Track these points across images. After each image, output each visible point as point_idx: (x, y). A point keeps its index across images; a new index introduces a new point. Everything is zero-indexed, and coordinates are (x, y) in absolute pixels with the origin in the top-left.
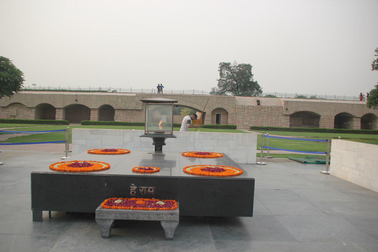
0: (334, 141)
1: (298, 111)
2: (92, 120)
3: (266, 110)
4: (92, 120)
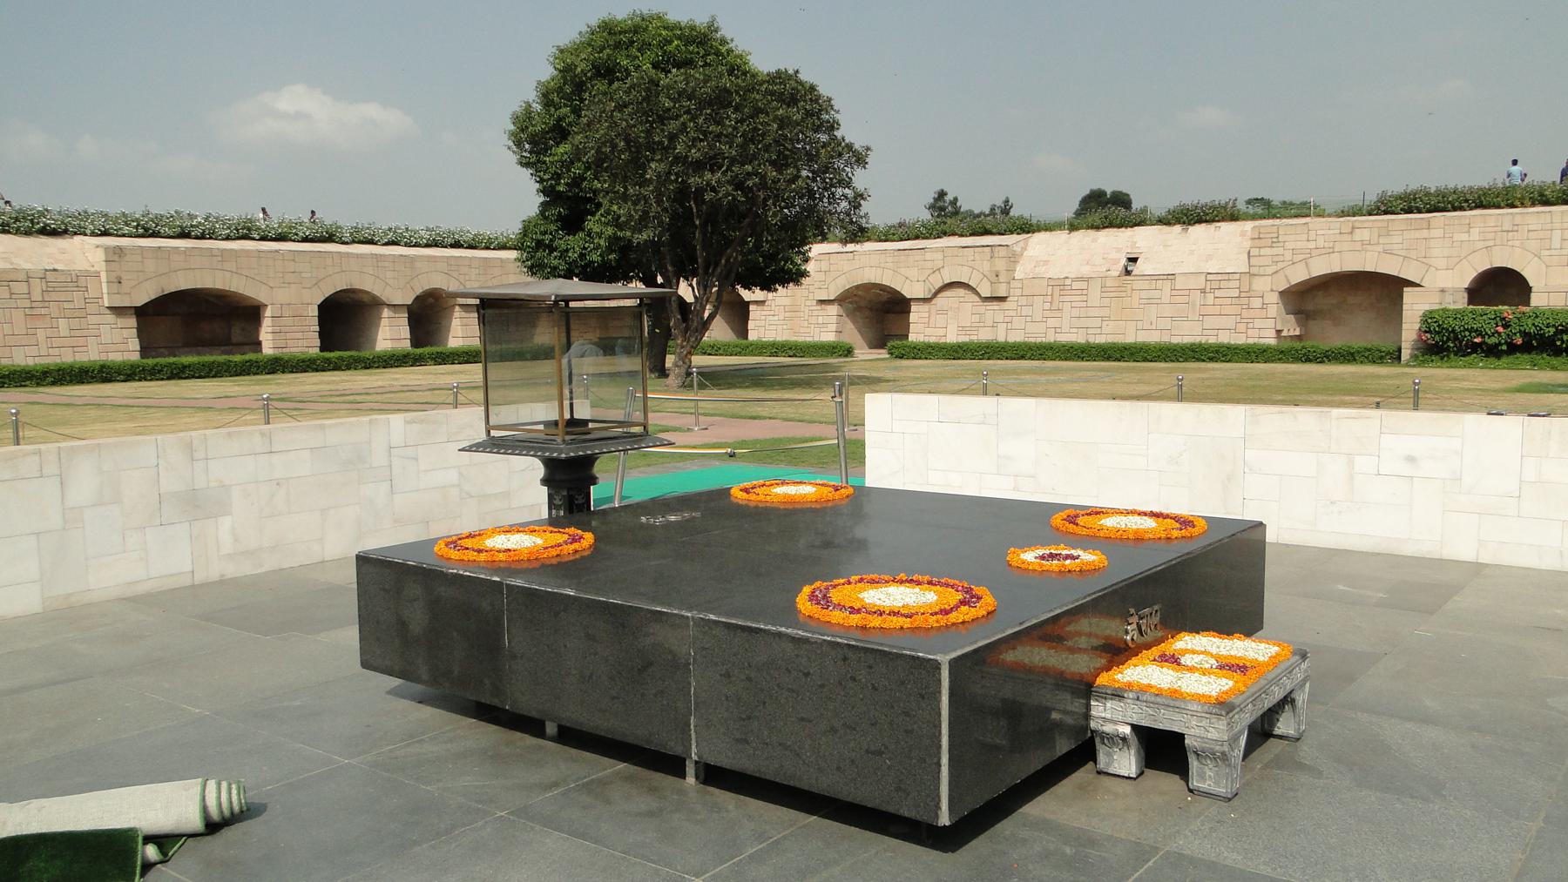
0: (867, 396)
1: (172, 288)
3: (21, 288)
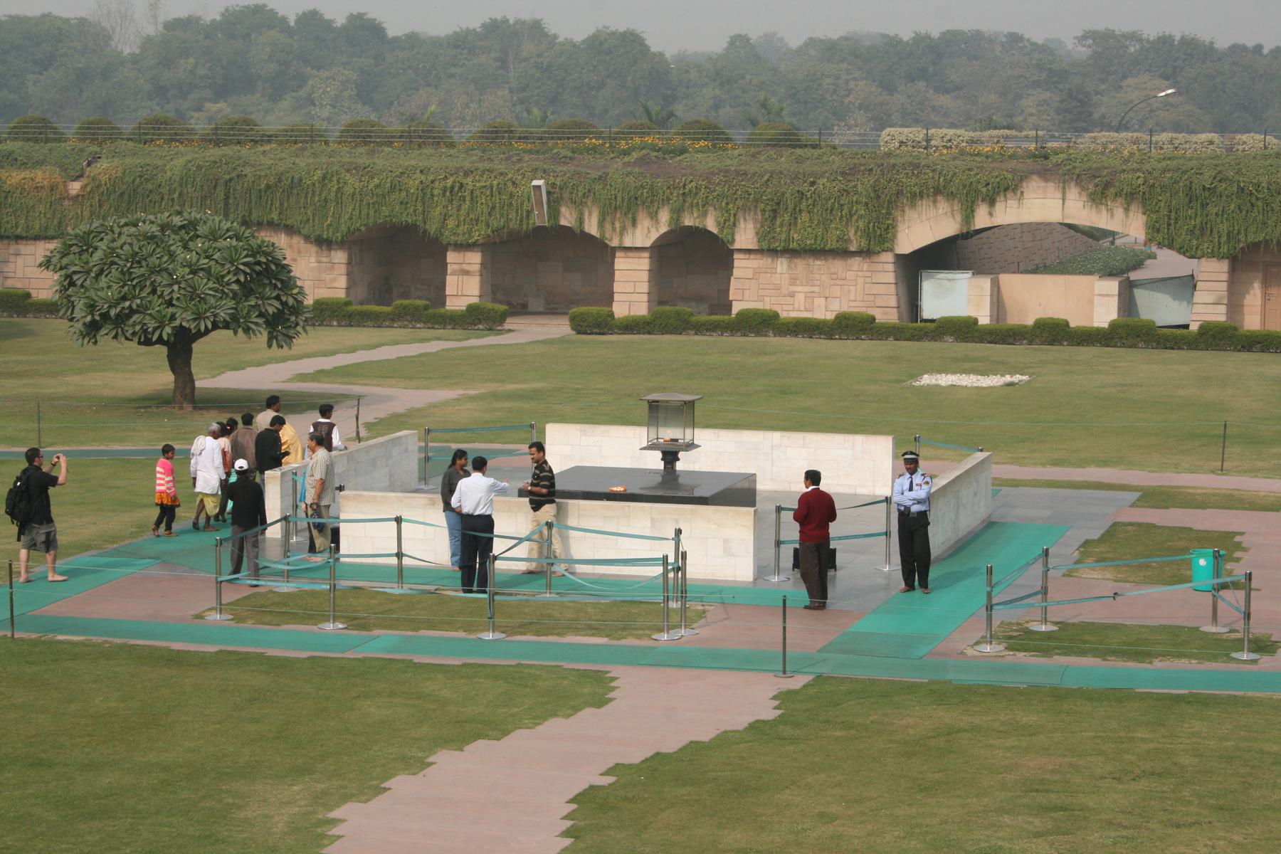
2: (620, 310)
4: (620, 310)
